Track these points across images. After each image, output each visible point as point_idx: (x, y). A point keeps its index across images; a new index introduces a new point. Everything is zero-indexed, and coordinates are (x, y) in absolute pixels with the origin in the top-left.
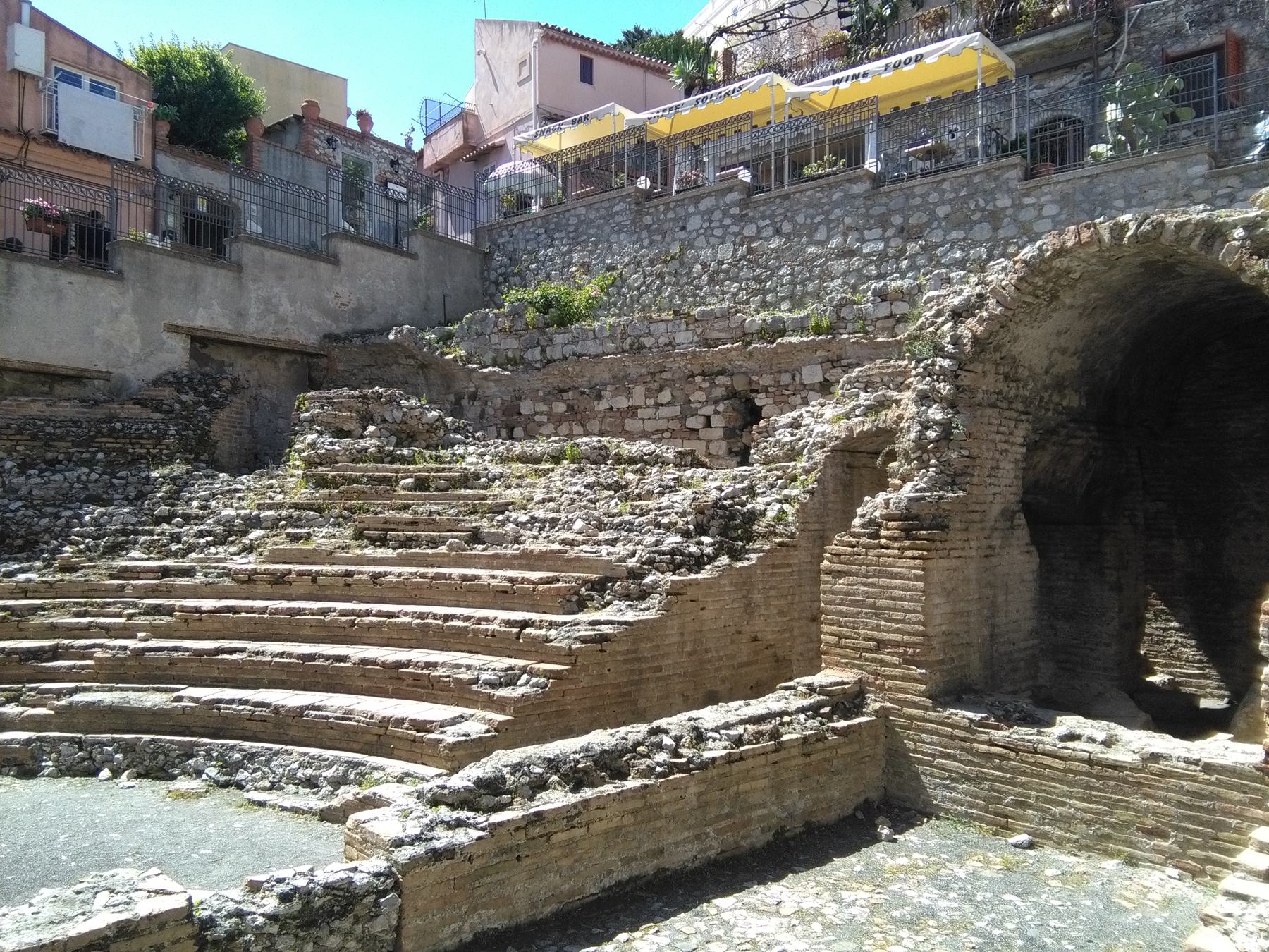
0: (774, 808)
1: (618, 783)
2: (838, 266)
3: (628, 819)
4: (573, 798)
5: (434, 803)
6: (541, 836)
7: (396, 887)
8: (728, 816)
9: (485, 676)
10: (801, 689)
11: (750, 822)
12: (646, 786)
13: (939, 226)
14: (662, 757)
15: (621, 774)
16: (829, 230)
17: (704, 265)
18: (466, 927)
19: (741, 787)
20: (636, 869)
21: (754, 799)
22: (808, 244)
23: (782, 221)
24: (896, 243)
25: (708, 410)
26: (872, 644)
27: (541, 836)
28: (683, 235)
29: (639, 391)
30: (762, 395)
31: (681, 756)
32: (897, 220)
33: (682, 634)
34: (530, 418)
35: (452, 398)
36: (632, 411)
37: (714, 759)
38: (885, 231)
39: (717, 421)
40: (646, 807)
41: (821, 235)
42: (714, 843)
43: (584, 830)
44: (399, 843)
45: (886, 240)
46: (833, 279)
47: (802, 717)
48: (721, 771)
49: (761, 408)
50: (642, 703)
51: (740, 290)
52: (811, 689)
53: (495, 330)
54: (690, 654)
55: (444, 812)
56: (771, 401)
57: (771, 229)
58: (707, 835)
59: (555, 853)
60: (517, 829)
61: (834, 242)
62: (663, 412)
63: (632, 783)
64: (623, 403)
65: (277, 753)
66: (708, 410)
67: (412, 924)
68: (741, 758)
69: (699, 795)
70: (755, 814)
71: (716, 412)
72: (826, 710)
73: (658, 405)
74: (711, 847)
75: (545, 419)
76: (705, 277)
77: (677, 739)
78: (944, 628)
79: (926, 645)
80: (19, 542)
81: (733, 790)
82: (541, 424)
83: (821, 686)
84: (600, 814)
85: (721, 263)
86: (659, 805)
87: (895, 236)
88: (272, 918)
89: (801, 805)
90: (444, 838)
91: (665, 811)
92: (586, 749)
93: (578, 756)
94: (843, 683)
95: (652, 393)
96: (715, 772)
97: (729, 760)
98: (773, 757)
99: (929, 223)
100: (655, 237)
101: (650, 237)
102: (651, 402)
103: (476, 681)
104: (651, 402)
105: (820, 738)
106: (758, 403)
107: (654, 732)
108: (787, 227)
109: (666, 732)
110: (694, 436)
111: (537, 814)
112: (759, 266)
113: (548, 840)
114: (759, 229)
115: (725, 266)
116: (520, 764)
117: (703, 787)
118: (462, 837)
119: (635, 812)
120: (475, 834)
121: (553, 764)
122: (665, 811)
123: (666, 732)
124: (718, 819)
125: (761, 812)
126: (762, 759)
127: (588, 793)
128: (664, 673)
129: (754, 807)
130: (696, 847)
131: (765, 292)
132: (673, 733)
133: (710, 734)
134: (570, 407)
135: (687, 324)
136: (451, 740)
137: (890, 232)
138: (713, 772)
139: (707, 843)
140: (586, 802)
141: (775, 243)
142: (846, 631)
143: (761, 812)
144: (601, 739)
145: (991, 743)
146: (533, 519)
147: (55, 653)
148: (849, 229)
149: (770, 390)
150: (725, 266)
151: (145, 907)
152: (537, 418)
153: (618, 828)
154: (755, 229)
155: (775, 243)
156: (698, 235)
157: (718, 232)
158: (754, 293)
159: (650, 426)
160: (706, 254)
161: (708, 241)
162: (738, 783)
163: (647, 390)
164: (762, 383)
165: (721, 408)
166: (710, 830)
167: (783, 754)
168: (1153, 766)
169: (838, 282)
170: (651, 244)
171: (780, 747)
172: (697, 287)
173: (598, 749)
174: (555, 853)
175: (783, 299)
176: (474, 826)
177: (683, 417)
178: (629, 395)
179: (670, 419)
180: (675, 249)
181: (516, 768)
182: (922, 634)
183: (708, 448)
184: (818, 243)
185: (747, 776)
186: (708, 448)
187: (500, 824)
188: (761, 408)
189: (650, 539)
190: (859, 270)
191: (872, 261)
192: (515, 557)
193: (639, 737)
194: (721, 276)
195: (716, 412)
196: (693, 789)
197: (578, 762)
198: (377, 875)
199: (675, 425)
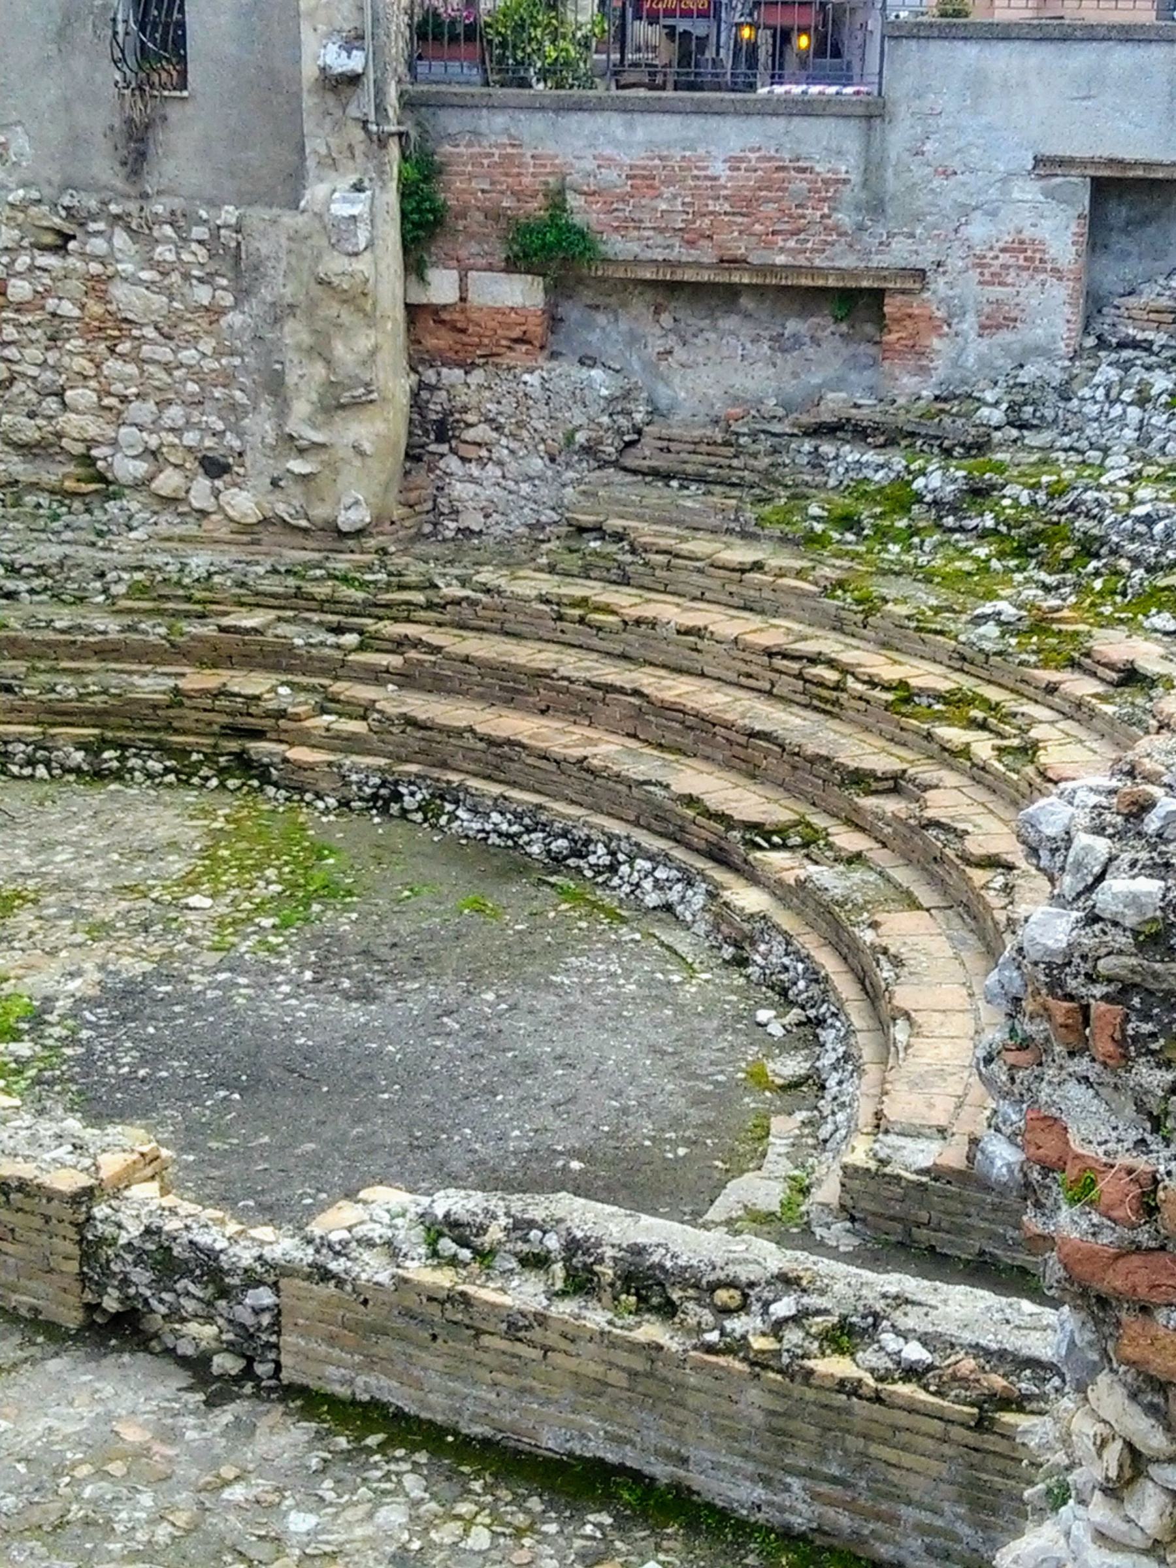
0: (964, 1530)
3: (617, 1378)
7: (275, 1286)
8: (834, 1480)
11: (893, 1519)
15: (668, 1310)
19: (874, 1449)
21: (917, 1486)
40: (650, 1375)
42: (801, 1506)
43: (537, 1354)
48: (824, 1398)
58: (787, 1488)
59: (486, 1358)
60: (431, 1299)
63: (652, 1330)
69: (773, 1413)
70: (904, 1510)
74: (792, 1510)
80: (1068, 552)
81: (854, 1443)
84: (563, 1344)
93: (609, 1252)
96: (810, 1394)
98: (971, 1438)
111: (463, 1294)
116: (532, 1224)
117: (779, 1406)
119: (633, 1374)
124: (807, 1473)
125: (925, 1517)
127: (565, 1308)
130: (759, 1493)
138: (797, 1389)
143: (925, 1517)
147: (895, 784)
166: (796, 1483)
171: (982, 1425)
174: (486, 1358)
193: (744, 1274)
197: (600, 1260)
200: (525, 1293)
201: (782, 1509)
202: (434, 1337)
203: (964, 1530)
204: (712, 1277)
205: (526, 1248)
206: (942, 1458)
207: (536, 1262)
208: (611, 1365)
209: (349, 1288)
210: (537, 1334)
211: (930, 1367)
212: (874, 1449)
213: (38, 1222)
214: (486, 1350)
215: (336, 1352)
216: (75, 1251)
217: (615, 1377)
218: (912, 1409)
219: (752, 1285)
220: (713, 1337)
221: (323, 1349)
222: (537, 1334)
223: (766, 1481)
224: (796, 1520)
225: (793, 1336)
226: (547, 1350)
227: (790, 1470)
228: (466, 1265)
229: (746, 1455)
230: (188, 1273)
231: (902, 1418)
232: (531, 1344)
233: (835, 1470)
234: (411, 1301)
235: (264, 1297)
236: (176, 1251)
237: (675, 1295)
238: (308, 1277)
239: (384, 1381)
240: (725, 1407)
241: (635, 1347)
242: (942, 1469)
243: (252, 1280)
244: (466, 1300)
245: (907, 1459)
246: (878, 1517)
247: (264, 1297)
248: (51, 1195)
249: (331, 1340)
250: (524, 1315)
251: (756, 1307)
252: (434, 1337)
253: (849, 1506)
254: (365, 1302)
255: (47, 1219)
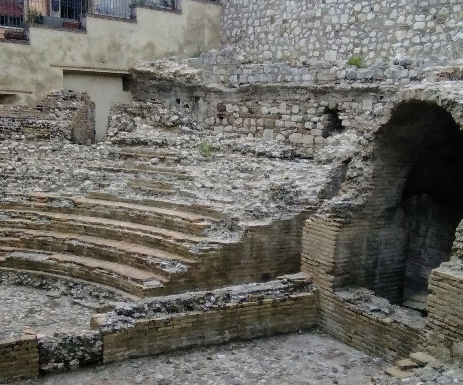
1: (188, 312)
2: (400, 35)
4: (169, 316)
5: (120, 313)
6: (154, 328)
7: (102, 339)
8: (234, 327)
9: (163, 263)
10: (285, 280)
11: (245, 330)
12: (198, 315)
13: (454, 17)
14: (208, 304)
15: (191, 309)
16: (398, 12)
17: (333, 26)
18: (126, 354)
19: (242, 317)
20: (192, 342)
22: (388, 19)
23: (375, 4)
24: (431, 24)
25: (316, 119)
26: (317, 264)
27: (154, 328)
28: (323, 5)
29: (283, 105)
30: (343, 113)
31: (216, 304)
32: (433, 11)
33: (252, 250)
34: (230, 115)
35: (194, 99)
36: (279, 116)
37: (229, 307)
38: (426, 17)
39: (320, 125)
41: (393, 15)
43: (171, 327)
44: (104, 326)
45: (426, 22)
46: (397, 42)
47: (278, 292)
49: (341, 121)
50: (230, 277)
51: (350, 42)
52: (289, 281)
53: (215, 63)
54: (255, 258)
55: (122, 317)
56: (346, 117)
57: (368, 8)
61: (401, 20)
62: (295, 118)
63: (192, 313)
64: (275, 110)
65: (86, 285)
66: (316, 119)
67: (106, 352)
68: (242, 307)
69: (222, 319)
70: (247, 327)
71: (320, 121)
72: (291, 289)
73: (291, 114)
74: (226, 337)
75: (237, 115)
76: (333, 33)
77: (217, 299)
78: (344, 261)
79: (335, 268)
81: (238, 318)
82: (236, 118)
83: (293, 280)
84: (178, 322)
85: (341, 25)
86: (204, 321)
87: (431, 20)
88: (60, 344)
89: (271, 325)
90: (120, 326)
91: (206, 323)
92: (178, 300)
93: (174, 302)
94: (304, 279)
95: (289, 107)
96: (229, 311)
97: (236, 307)
99: (450, 14)
100: (308, 5)
101: (306, 5)
102: (288, 112)
103: (158, 264)
104: (288, 112)
105: (284, 300)
106: (340, 117)
107: (211, 294)
108: (376, 7)
109: (213, 295)
110: (308, 132)
111: (153, 321)
112: (360, 30)
113: (157, 330)
114: (363, 7)
115: (343, 28)
116: (151, 304)
118: (125, 326)
120: (129, 325)
121: (163, 304)
122: (206, 323)
123: (213, 295)
124: (230, 328)
125: (251, 327)
126: (252, 308)
127: (175, 315)
128: (242, 265)
129: (248, 325)
130: (220, 337)
131: (363, 46)
132: (216, 296)
133: (233, 297)
134: (251, 111)
135: (309, 70)
136: (144, 287)
137: (429, 17)
138: (228, 311)
139: (224, 336)
140: (172, 319)
141: (371, 16)
142: (309, 257)
143: (251, 327)
144: (186, 296)
145: (349, 309)
146: (204, 187)
148: (408, 13)
149: (347, 111)
150: (343, 28)
151: (24, 338)
152: (234, 114)
153: (186, 328)
154: (361, 7)
155: (371, 16)
156: (331, 7)
157: (341, 6)
158: (356, 45)
159: (288, 124)
160: (335, 20)
161: (336, 11)
162: (240, 315)
163: (287, 105)
164: (343, 107)
165: (322, 118)
166: (226, 331)
167: (262, 306)
168: (394, 325)
169: (399, 44)
170: (307, 8)
171: (261, 303)
172: (329, 39)
173: (183, 300)
174: (158, 333)
175: (370, 51)
176: (130, 323)
177: (304, 121)
178: (278, 107)
179: (297, 122)
180: (319, 13)
181: (150, 305)
182: (333, 263)
183: (314, 140)
184: (392, 19)
185: (244, 313)
186: (314, 140)
187: (139, 323)
188: (341, 121)
189: (248, 203)
190: (410, 39)
191: (418, 34)
192: (190, 207)
193: (202, 296)
194: (341, 33)
195: (320, 121)
196: (219, 316)
197: (173, 304)
198: (95, 335)
199: (299, 125)
200: (162, 317)
201: (224, 338)
202: (146, 335)
203: (257, 326)
204: (197, 299)
205: (153, 309)
206: (253, 313)
207: (158, 310)
208: (188, 323)
209: (123, 331)
210: (171, 323)
211: (245, 299)
212: (242, 317)
213: (24, 351)
214: (159, 332)
215: (120, 349)
216: (37, 354)
217: (190, 325)
218: (248, 306)
219: (204, 298)
220: (206, 309)
221: (116, 350)
222: (171, 323)
223: (220, 334)
224: (226, 339)
225: (219, 303)
226: (173, 325)
227: (225, 330)
228: (145, 317)
229: (216, 330)
230: (78, 346)
231: (246, 309)
232: (170, 326)
233: (234, 325)
234: (140, 328)
235: (99, 343)
236: (74, 341)
237: (191, 305)
238: (112, 333)
239: (133, 351)
240: (213, 321)
241: (193, 317)
242: (254, 315)
243: (95, 340)
244: (154, 322)
245: (247, 316)
246: (242, 331)
247: (99, 343)
248: (28, 342)
249: (118, 347)
250: (168, 319)
251: (207, 301)
252: (146, 335)
253: (238, 332)
254: (127, 333)
255: (27, 349)
